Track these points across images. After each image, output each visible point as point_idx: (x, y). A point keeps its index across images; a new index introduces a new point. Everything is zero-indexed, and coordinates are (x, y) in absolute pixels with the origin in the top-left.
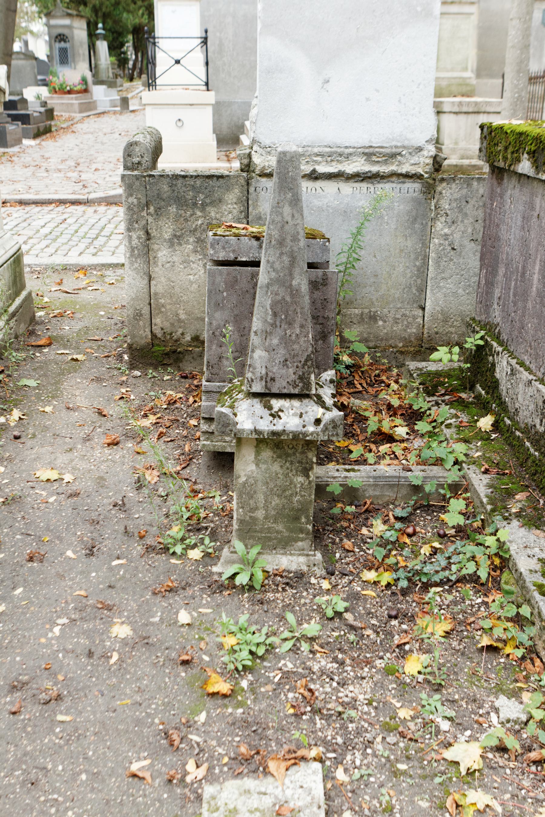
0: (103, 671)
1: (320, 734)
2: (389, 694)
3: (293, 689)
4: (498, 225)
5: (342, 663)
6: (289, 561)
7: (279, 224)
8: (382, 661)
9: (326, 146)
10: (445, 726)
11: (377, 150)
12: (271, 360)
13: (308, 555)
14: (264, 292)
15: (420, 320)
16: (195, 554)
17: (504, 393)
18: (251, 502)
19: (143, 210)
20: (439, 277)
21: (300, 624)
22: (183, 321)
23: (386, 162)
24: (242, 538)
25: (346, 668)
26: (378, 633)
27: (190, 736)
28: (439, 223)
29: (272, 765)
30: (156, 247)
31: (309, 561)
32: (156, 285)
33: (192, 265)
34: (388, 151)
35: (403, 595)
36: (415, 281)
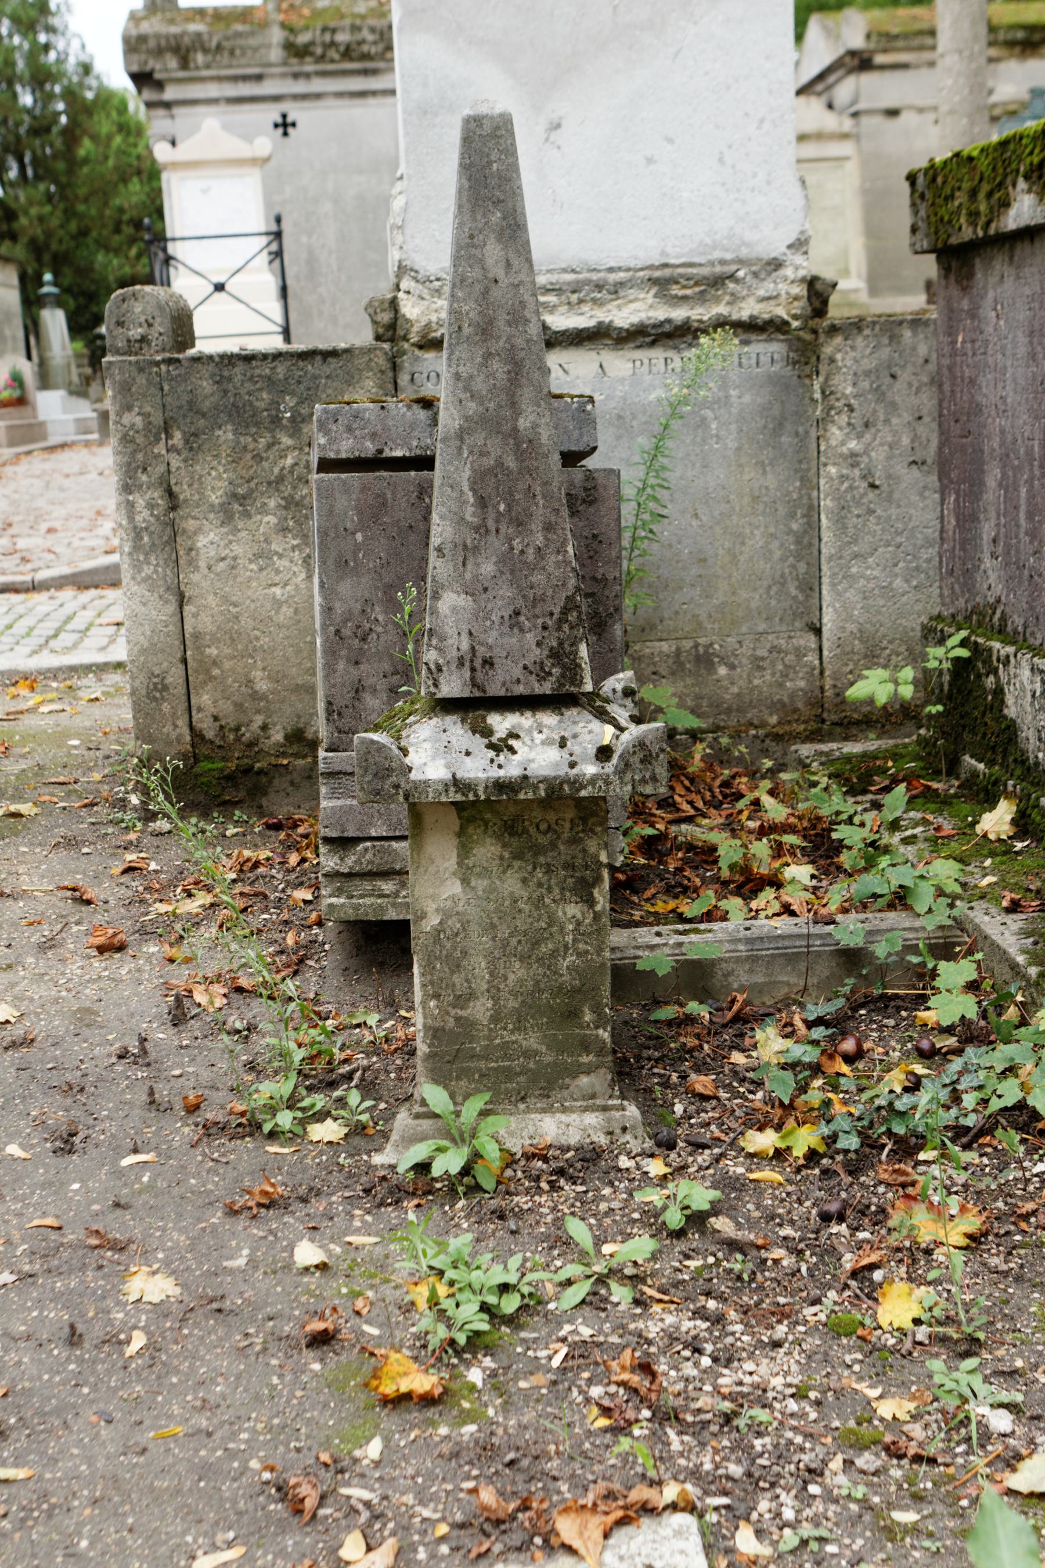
0: (109, 1372)
1: (682, 1462)
2: (846, 1373)
3: (602, 1377)
4: (972, 382)
5: (718, 1320)
6: (559, 1127)
7: (478, 287)
8: (816, 1308)
9: (564, 271)
10: (1001, 1422)
11: (680, 270)
12: (481, 614)
13: (605, 1109)
14: (453, 450)
15: (812, 658)
16: (328, 1131)
17: (1033, 744)
18: (457, 979)
19: (158, 440)
20: (847, 553)
21: (599, 1242)
22: (264, 697)
23: (701, 298)
24: (439, 1078)
25: (730, 1328)
26: (800, 1253)
27: (344, 1491)
28: (834, 430)
29: (567, 1528)
30: (191, 525)
31: (609, 1120)
32: (195, 616)
33: (279, 563)
34: (705, 271)
35: (850, 1173)
36: (794, 567)
